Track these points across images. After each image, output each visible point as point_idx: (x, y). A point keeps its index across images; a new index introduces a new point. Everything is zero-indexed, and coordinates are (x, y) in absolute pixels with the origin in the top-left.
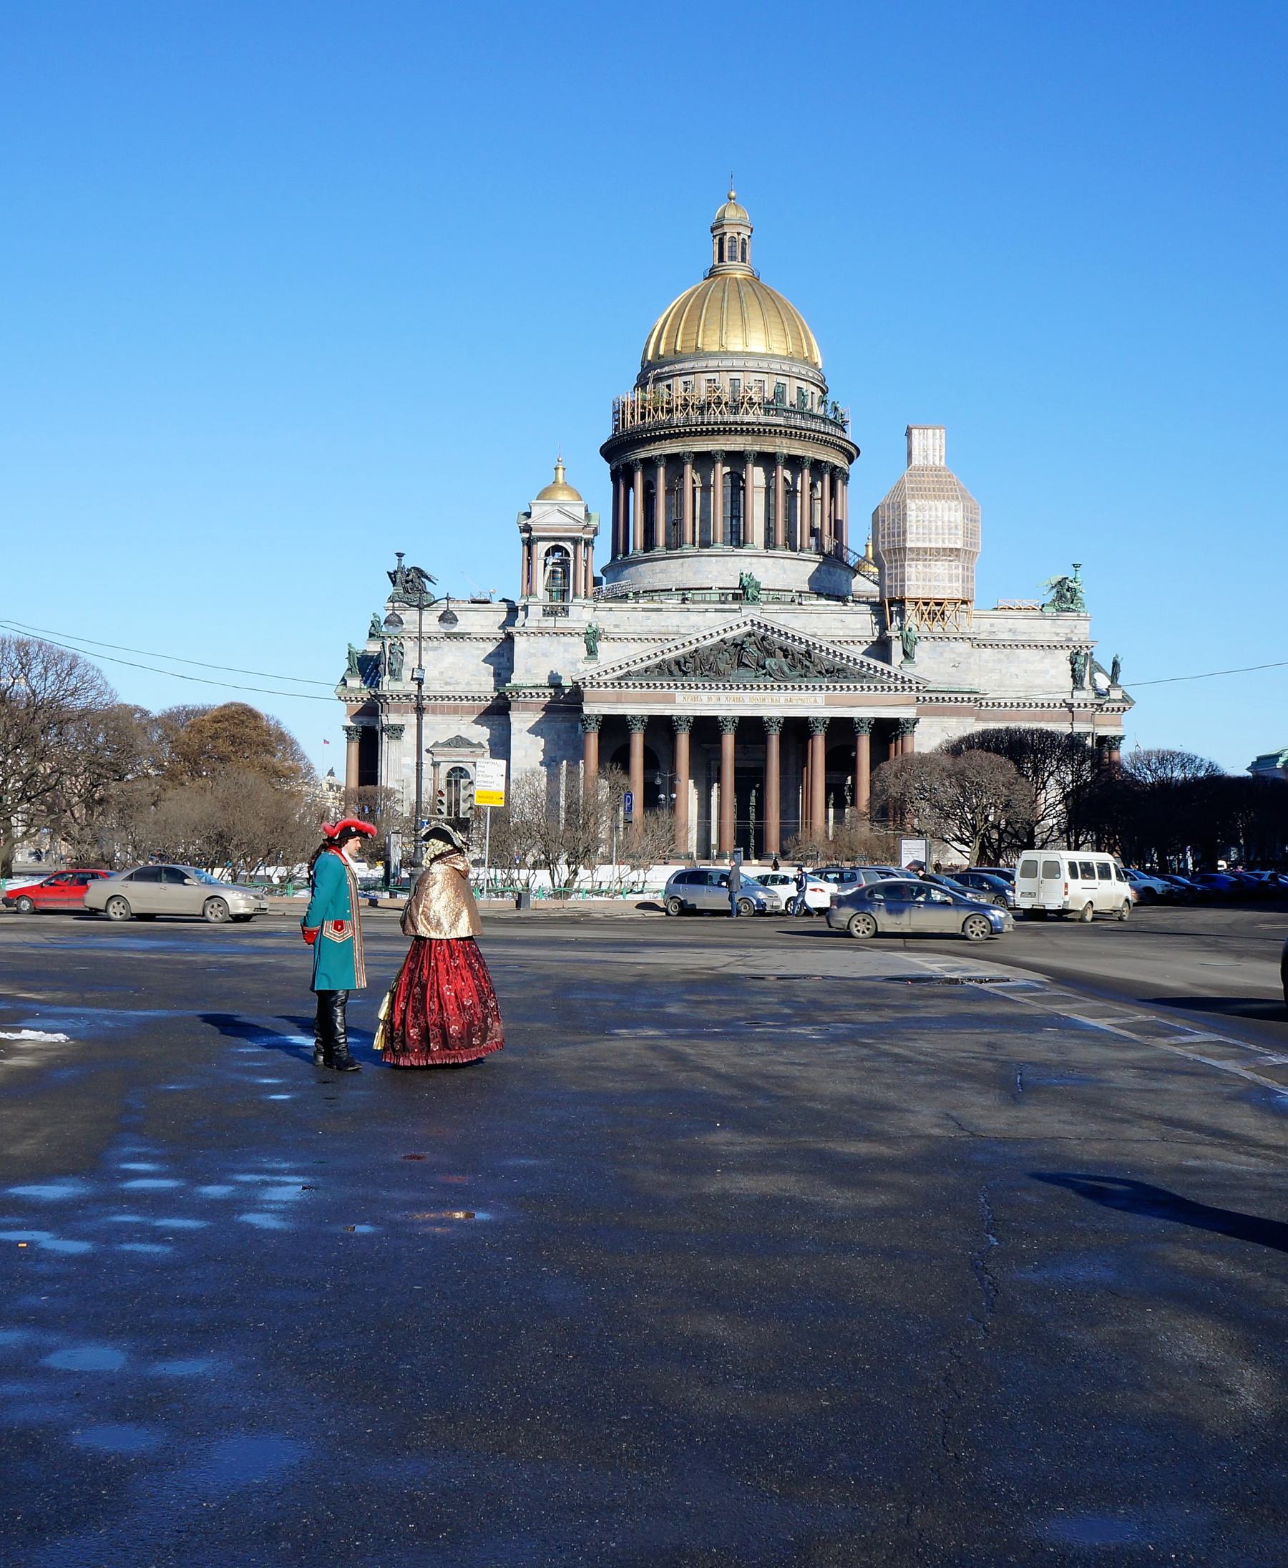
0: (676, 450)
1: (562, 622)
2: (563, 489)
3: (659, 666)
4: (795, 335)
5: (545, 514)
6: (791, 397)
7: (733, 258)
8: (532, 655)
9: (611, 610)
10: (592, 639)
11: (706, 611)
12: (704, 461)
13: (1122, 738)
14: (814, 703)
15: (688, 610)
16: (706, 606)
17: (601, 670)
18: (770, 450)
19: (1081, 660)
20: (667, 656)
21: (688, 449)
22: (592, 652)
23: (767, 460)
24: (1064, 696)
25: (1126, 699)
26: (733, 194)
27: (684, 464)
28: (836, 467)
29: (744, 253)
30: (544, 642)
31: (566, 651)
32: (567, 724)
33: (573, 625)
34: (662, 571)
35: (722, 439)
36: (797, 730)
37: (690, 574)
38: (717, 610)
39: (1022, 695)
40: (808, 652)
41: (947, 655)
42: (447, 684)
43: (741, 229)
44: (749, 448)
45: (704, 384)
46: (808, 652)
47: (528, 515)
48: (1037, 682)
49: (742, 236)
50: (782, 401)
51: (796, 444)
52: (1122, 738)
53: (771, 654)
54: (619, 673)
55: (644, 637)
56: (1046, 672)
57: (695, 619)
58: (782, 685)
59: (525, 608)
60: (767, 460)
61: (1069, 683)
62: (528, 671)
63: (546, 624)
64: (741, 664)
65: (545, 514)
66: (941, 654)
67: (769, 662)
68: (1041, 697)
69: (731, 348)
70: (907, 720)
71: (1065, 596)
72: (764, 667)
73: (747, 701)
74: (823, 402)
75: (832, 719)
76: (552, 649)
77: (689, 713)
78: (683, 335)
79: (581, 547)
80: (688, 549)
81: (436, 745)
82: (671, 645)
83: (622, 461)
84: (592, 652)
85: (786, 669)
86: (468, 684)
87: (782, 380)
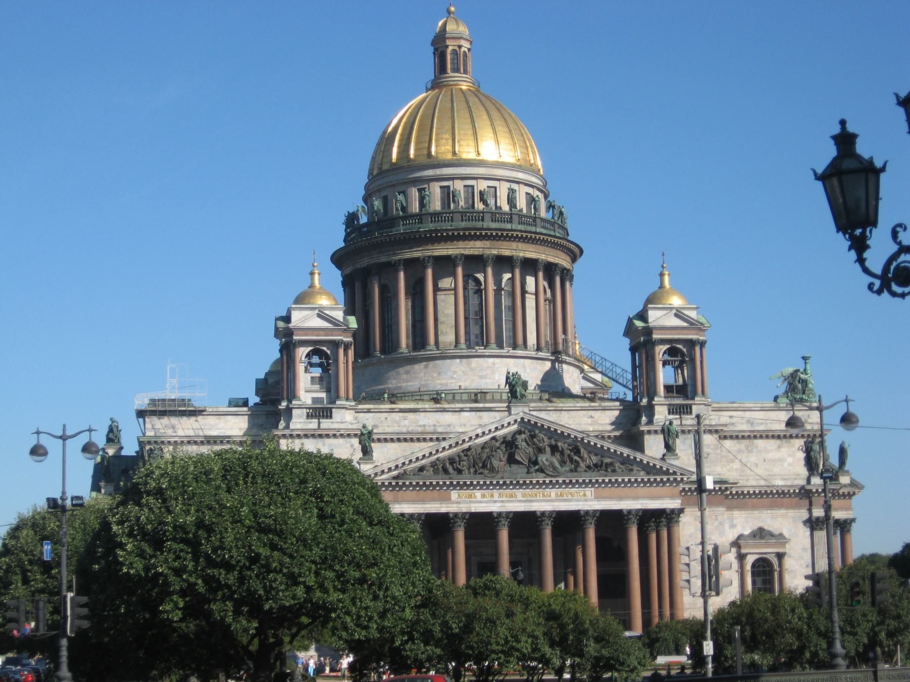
1: (326, 424)
2: (320, 293)
3: (433, 465)
4: (523, 144)
5: (306, 319)
6: (522, 203)
7: (456, 70)
9: (369, 411)
10: (366, 439)
11: (462, 410)
13: (853, 520)
14: (585, 500)
15: (444, 410)
16: (461, 405)
17: (378, 470)
18: (507, 253)
19: (816, 447)
20: (440, 455)
22: (366, 452)
24: (803, 482)
25: (853, 484)
26: (452, 9)
27: (425, 268)
28: (565, 269)
29: (465, 65)
33: (336, 426)
34: (407, 373)
35: (461, 244)
36: (568, 524)
37: (435, 375)
38: (472, 410)
39: (763, 483)
43: (463, 43)
44: (487, 252)
45: (438, 191)
47: (287, 319)
48: (776, 470)
49: (463, 49)
51: (531, 247)
52: (853, 520)
53: (540, 450)
54: (395, 473)
55: (402, 437)
56: (782, 460)
57: (448, 418)
58: (554, 480)
59: (289, 411)
60: (504, 263)
61: (804, 472)
64: (512, 460)
65: (306, 319)
67: (543, 459)
68: (779, 482)
69: (465, 156)
70: (673, 511)
71: (796, 388)
72: (536, 463)
73: (520, 497)
74: (550, 206)
77: (464, 510)
78: (417, 144)
79: (341, 351)
82: (445, 444)
83: (358, 266)
84: (366, 452)
85: (557, 465)
87: (515, 186)
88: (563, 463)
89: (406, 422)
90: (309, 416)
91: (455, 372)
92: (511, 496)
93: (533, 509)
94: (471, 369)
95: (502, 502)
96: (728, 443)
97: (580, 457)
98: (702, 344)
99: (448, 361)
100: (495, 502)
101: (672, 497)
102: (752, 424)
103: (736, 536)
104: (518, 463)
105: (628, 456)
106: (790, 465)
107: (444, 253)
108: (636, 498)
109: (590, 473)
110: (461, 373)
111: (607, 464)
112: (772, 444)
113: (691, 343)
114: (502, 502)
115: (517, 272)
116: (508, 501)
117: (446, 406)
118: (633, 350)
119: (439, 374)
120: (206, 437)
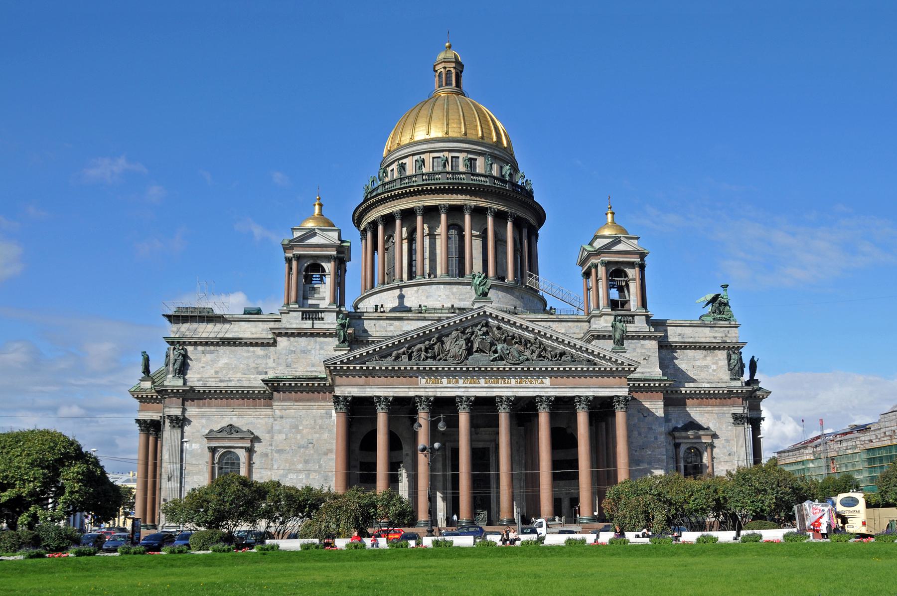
0: (411, 206)
1: (318, 324)
8: (294, 352)
12: (431, 213)
13: (763, 419)
15: (425, 319)
18: (484, 205)
19: (734, 357)
21: (421, 204)
23: (479, 213)
24: (724, 385)
28: (531, 225)
30: (303, 341)
31: (321, 348)
32: (323, 411)
33: (327, 326)
36: (524, 411)
37: (424, 298)
41: (638, 350)
42: (221, 381)
44: (467, 203)
52: (763, 419)
56: (707, 367)
62: (288, 365)
63: (305, 326)
66: (634, 350)
68: (708, 385)
72: (495, 352)
75: (558, 399)
76: (309, 348)
77: (430, 394)
80: (418, 279)
81: (211, 431)
86: (240, 380)
88: (520, 353)
89: (392, 328)
90: (302, 319)
91: (440, 296)
93: (494, 394)
94: (453, 294)
95: (466, 387)
96: (664, 352)
98: (642, 267)
99: (434, 286)
100: (459, 387)
101: (620, 386)
102: (683, 337)
103: (671, 428)
104: (480, 350)
106: (714, 371)
107: (433, 203)
108: (588, 386)
110: (444, 297)
111: (563, 354)
112: (699, 354)
113: (632, 265)
114: (466, 387)
115: (490, 220)
117: (426, 315)
118: (587, 274)
119: (427, 297)
120: (221, 339)
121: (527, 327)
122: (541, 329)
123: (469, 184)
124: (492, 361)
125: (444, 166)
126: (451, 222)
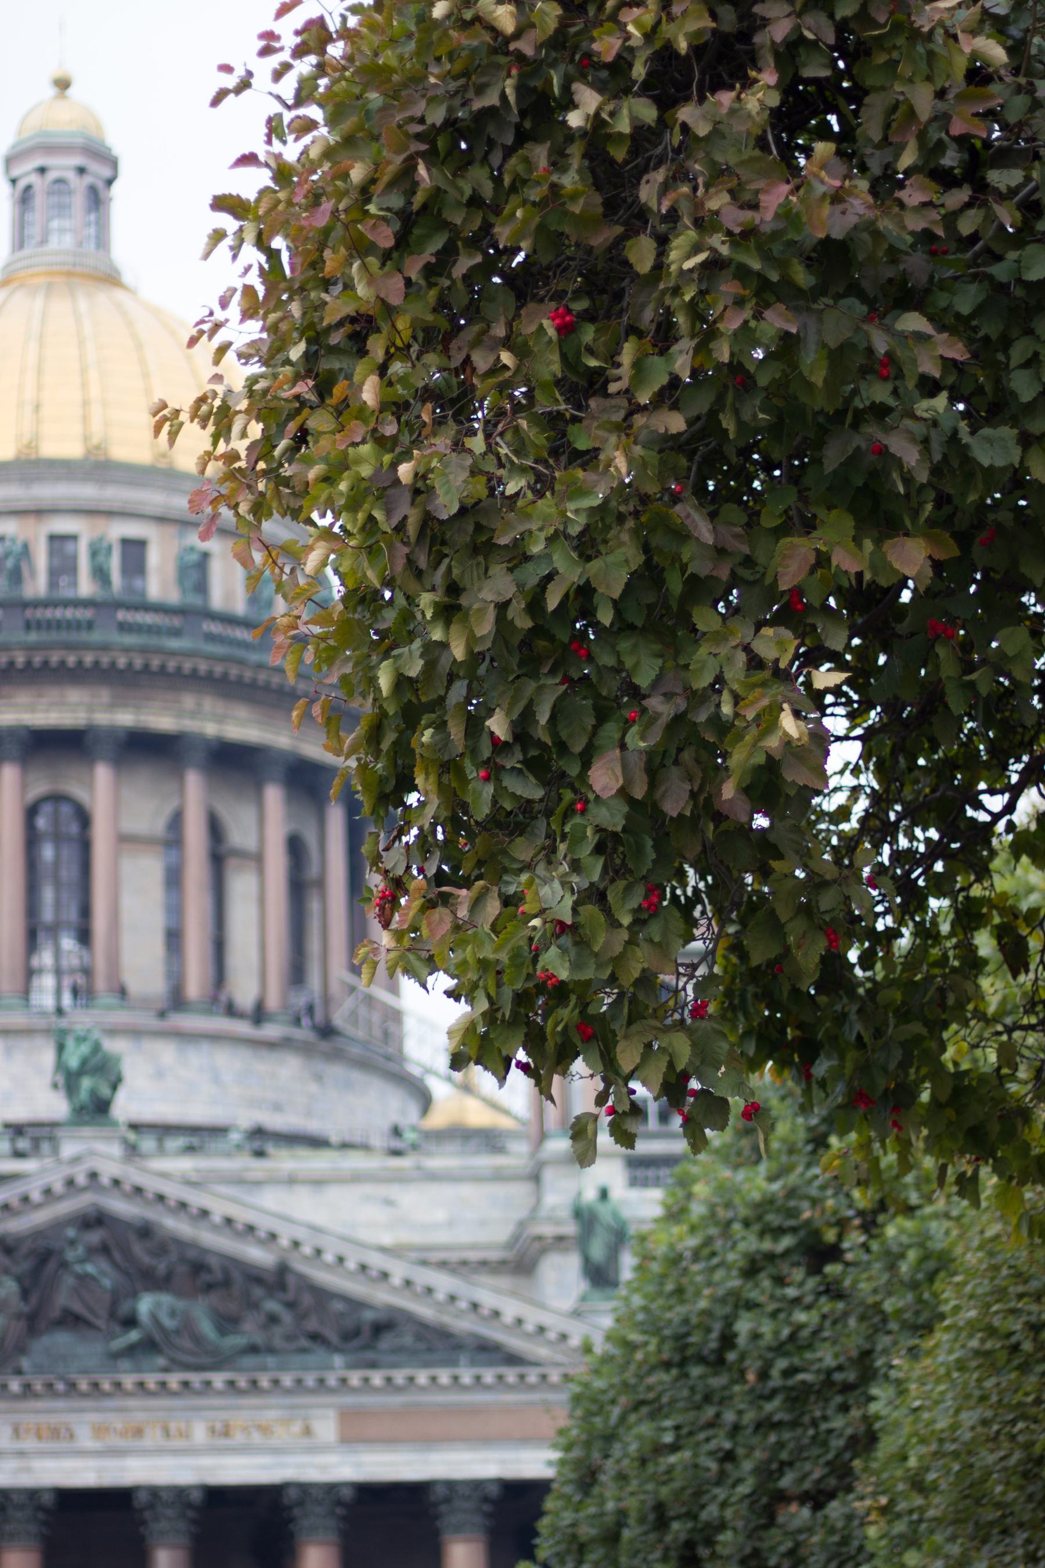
40: (283, 1269)
44: (103, 718)
46: (283, 1269)
49: (88, 180)
50: (202, 587)
51: (242, 711)
58: (195, 1378)
69: (51, 449)
72: (131, 1322)
73: (86, 1440)
88: (227, 1323)
92: (55, 1433)
97: (291, 1305)
104: (71, 1320)
105: (453, 1298)
109: (319, 1355)
114: (21, 1454)
115: (194, 782)
116: (42, 1454)
121: (251, 1229)
122: (301, 1234)
123: (105, 648)
124: (116, 1356)
125: (16, 577)
126: (40, 788)
